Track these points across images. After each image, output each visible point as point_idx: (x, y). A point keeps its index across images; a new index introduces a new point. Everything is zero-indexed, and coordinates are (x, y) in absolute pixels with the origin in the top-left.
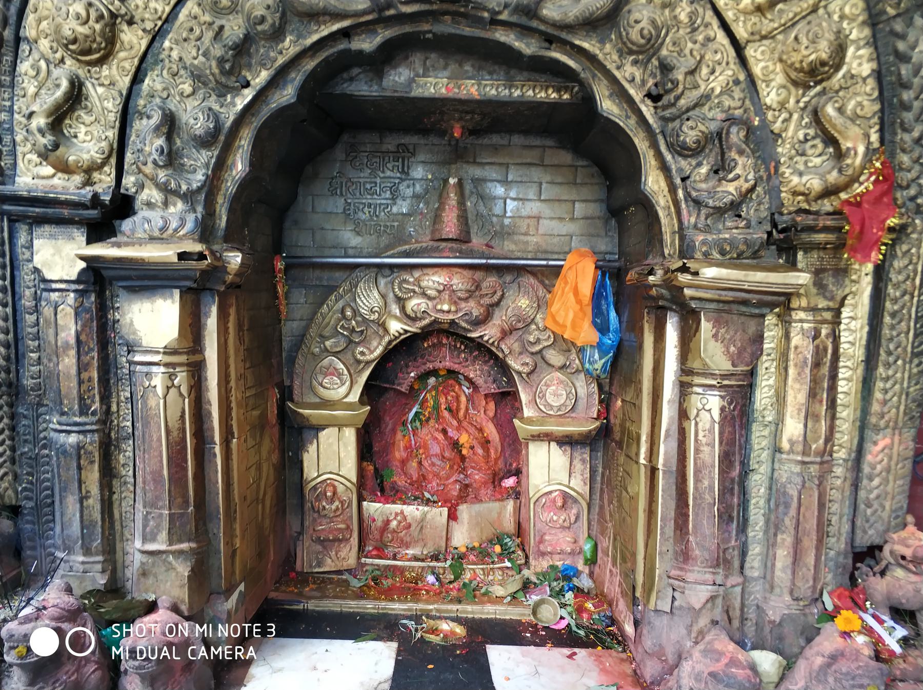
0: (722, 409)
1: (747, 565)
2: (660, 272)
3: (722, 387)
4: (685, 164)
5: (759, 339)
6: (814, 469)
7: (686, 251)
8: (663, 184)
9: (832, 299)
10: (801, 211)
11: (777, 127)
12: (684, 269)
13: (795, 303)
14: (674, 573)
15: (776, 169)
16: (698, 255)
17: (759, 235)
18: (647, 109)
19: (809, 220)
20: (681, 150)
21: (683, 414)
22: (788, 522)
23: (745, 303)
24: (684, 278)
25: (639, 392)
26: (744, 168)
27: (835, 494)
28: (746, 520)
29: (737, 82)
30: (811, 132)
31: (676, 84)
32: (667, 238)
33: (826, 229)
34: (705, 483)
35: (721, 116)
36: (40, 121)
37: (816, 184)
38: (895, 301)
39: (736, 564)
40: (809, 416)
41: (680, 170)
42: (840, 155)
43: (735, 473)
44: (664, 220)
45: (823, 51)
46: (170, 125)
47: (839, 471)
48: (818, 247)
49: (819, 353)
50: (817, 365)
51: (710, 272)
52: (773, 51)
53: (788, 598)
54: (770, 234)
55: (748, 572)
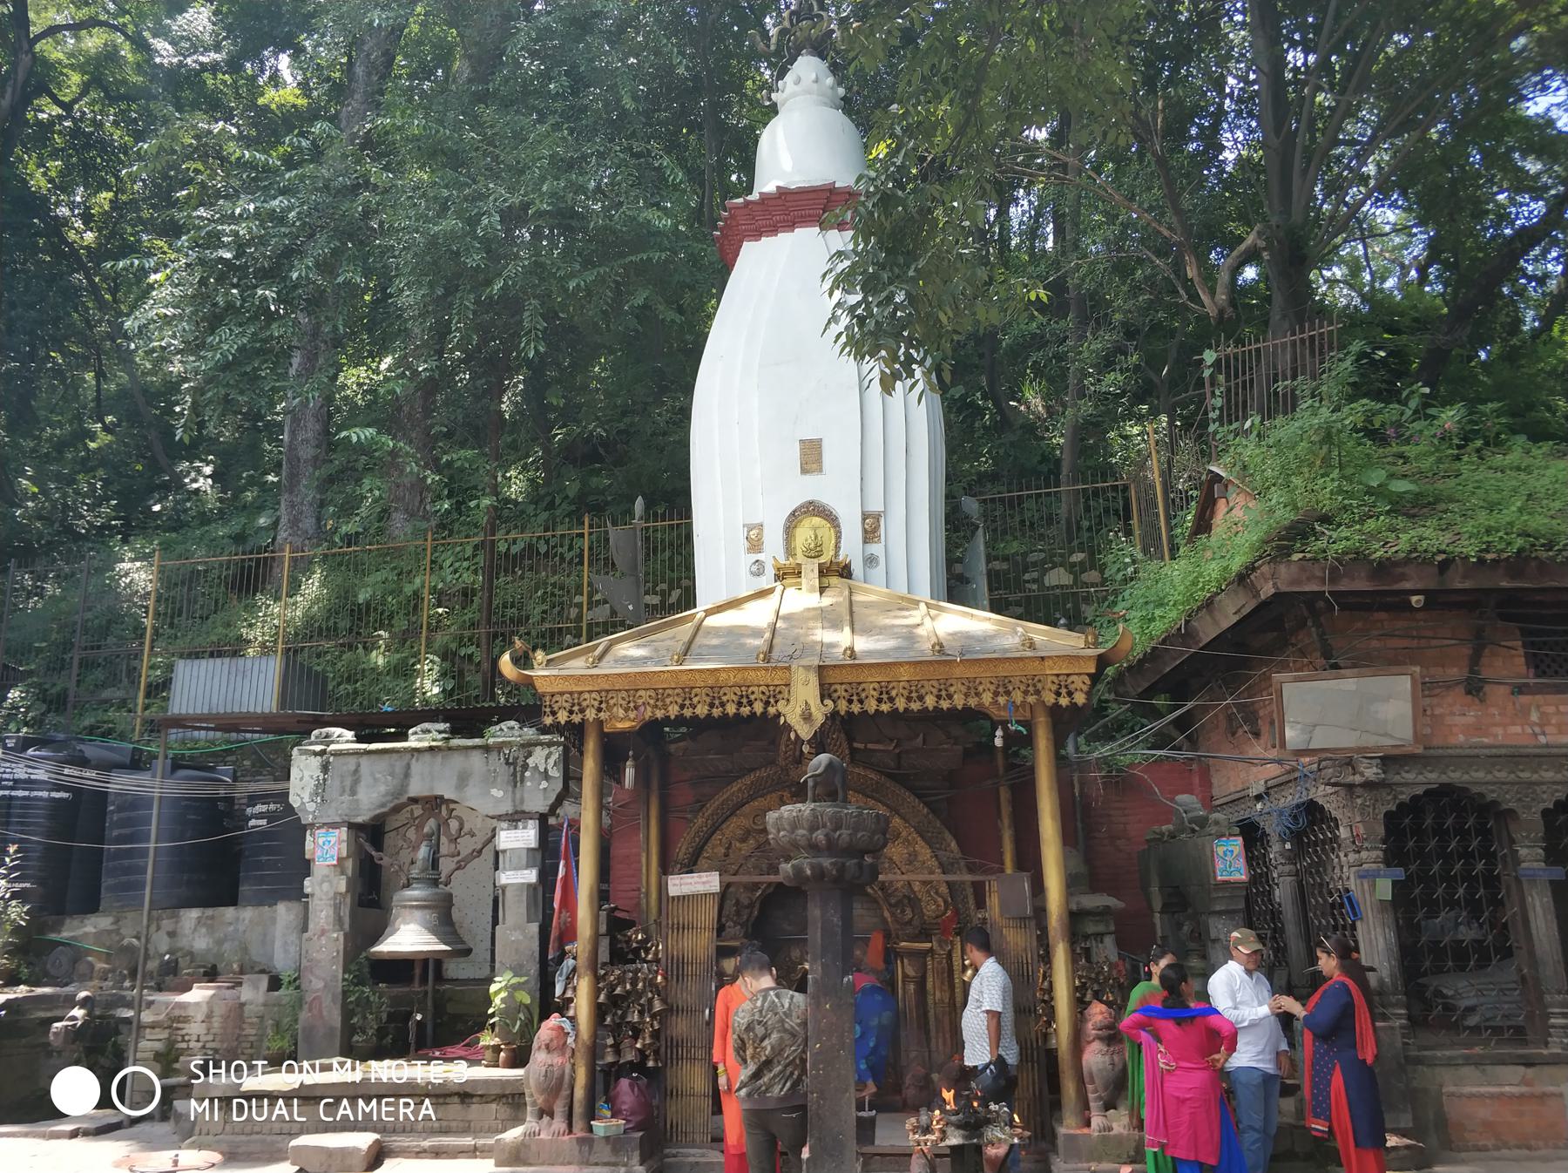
26: (908, 911)
46: (738, 902)
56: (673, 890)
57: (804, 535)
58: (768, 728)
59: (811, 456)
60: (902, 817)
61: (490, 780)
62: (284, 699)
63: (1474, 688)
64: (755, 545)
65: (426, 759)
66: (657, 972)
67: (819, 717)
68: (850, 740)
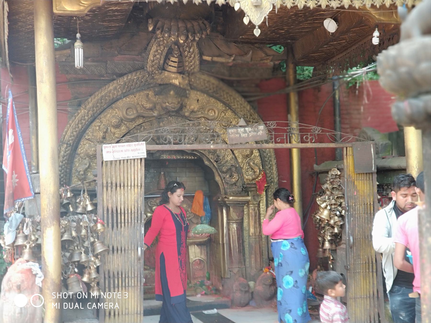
0: (237, 228)
1: (246, 264)
2: (221, 198)
3: (236, 223)
4: (224, 175)
5: (243, 211)
6: (257, 239)
7: (226, 193)
8: (220, 179)
9: (257, 202)
10: (248, 184)
11: (242, 166)
12: (226, 198)
13: (250, 203)
14: (230, 267)
15: (243, 175)
16: (228, 194)
17: (241, 190)
18: (215, 164)
19: (250, 186)
20: (223, 172)
21: (229, 230)
22: (253, 252)
23: (239, 204)
24: (226, 199)
25: (218, 226)
26: (235, 175)
27: (263, 246)
28: (245, 253)
29: (233, 158)
30: (249, 167)
31: (221, 159)
32: (222, 190)
33: (253, 187)
34: (235, 244)
35: (230, 165)
36: (82, 173)
37: (251, 178)
38: (270, 201)
39: (243, 263)
40: (255, 228)
41: (223, 176)
42: (255, 172)
43: (241, 242)
44: (220, 187)
45: (248, 152)
47: (263, 240)
48: (252, 191)
49: (255, 213)
50: (255, 216)
51: (231, 198)
52: (239, 152)
53: (255, 270)
54: (242, 189)
55: (246, 266)
56: (107, 157)
60: (234, 112)
66: (96, 222)
68: (201, 54)
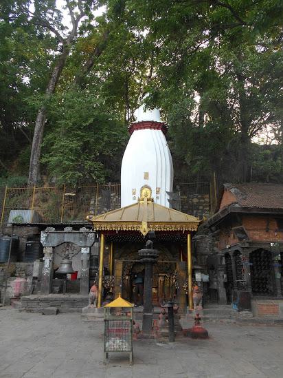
57: (144, 191)
58: (138, 233)
59: (146, 176)
61: (81, 239)
62: (33, 219)
63: (267, 231)
64: (134, 193)
65: (68, 236)
67: (147, 231)
